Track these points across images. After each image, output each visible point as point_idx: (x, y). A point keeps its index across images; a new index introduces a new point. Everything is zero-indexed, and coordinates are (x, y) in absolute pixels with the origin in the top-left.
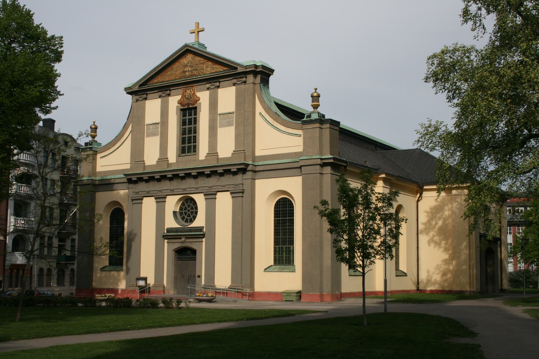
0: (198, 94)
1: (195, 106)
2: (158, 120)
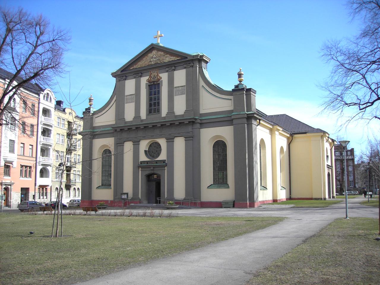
0: (161, 75)
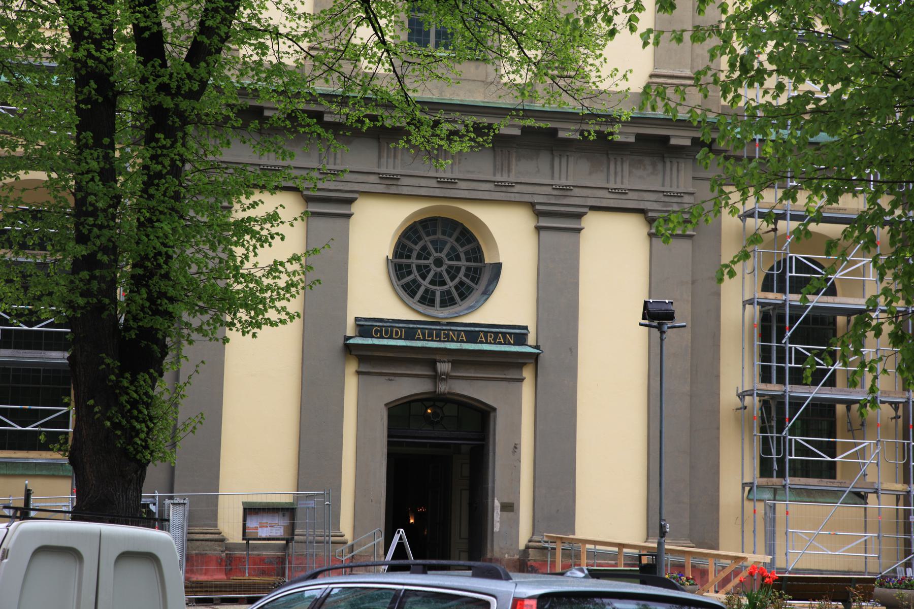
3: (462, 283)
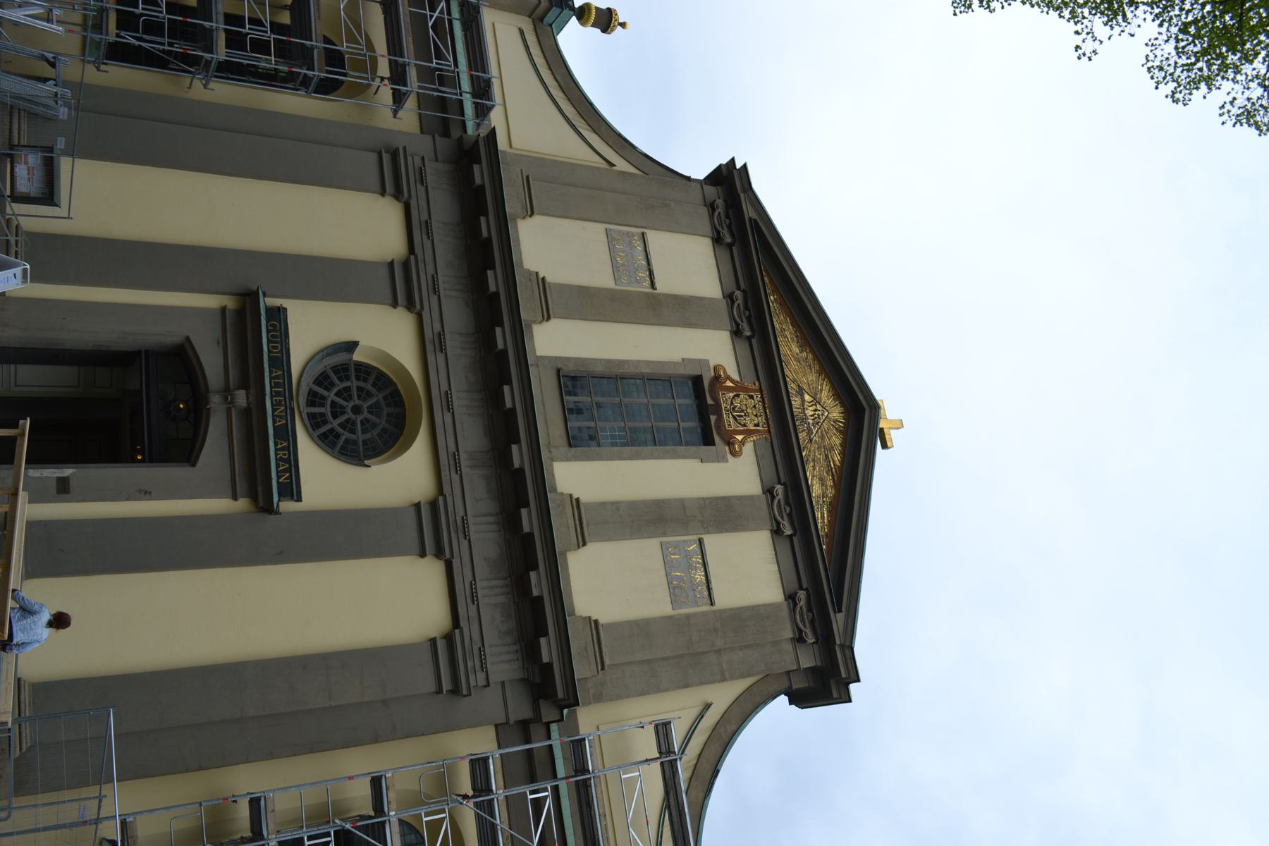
1: (717, 438)
2: (663, 286)
3: (338, 436)
